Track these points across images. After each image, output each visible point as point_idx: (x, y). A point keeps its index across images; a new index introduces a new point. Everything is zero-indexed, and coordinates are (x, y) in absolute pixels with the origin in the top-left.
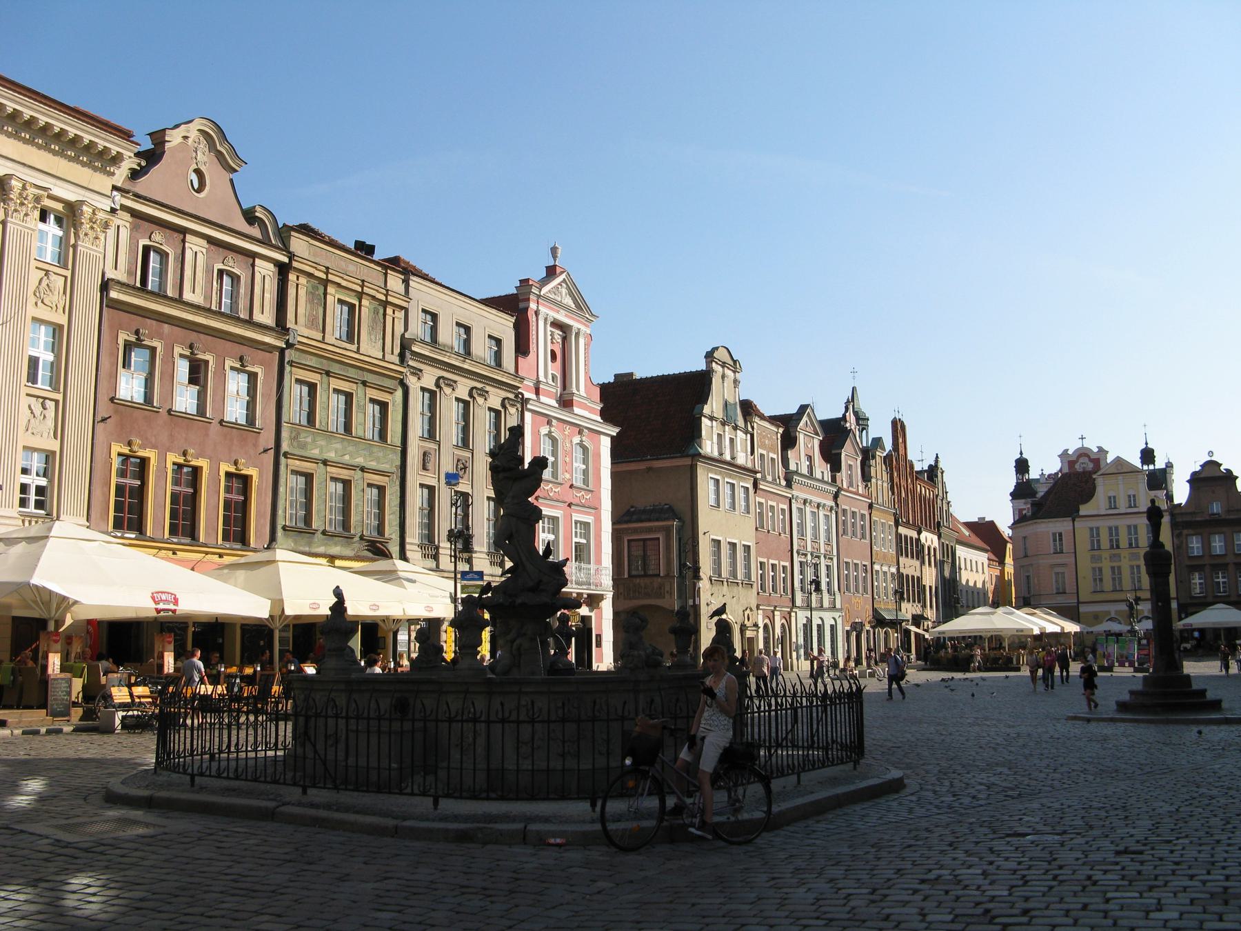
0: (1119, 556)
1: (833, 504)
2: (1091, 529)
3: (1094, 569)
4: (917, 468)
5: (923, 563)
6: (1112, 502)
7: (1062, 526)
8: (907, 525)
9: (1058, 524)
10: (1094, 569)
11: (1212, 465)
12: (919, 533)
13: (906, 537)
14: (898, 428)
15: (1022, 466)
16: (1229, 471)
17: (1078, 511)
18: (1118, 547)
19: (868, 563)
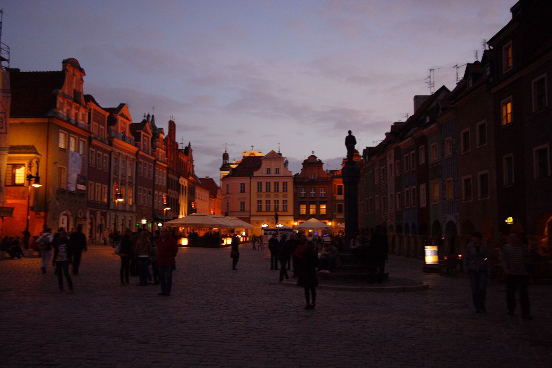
0: (270, 195)
1: (135, 158)
2: (258, 183)
3: (258, 201)
4: (180, 147)
5: (179, 193)
6: (269, 170)
7: (245, 180)
10: (258, 201)
11: (313, 157)
12: (179, 178)
13: (172, 179)
14: (172, 125)
15: (226, 156)
16: (320, 161)
17: (253, 174)
18: (269, 191)
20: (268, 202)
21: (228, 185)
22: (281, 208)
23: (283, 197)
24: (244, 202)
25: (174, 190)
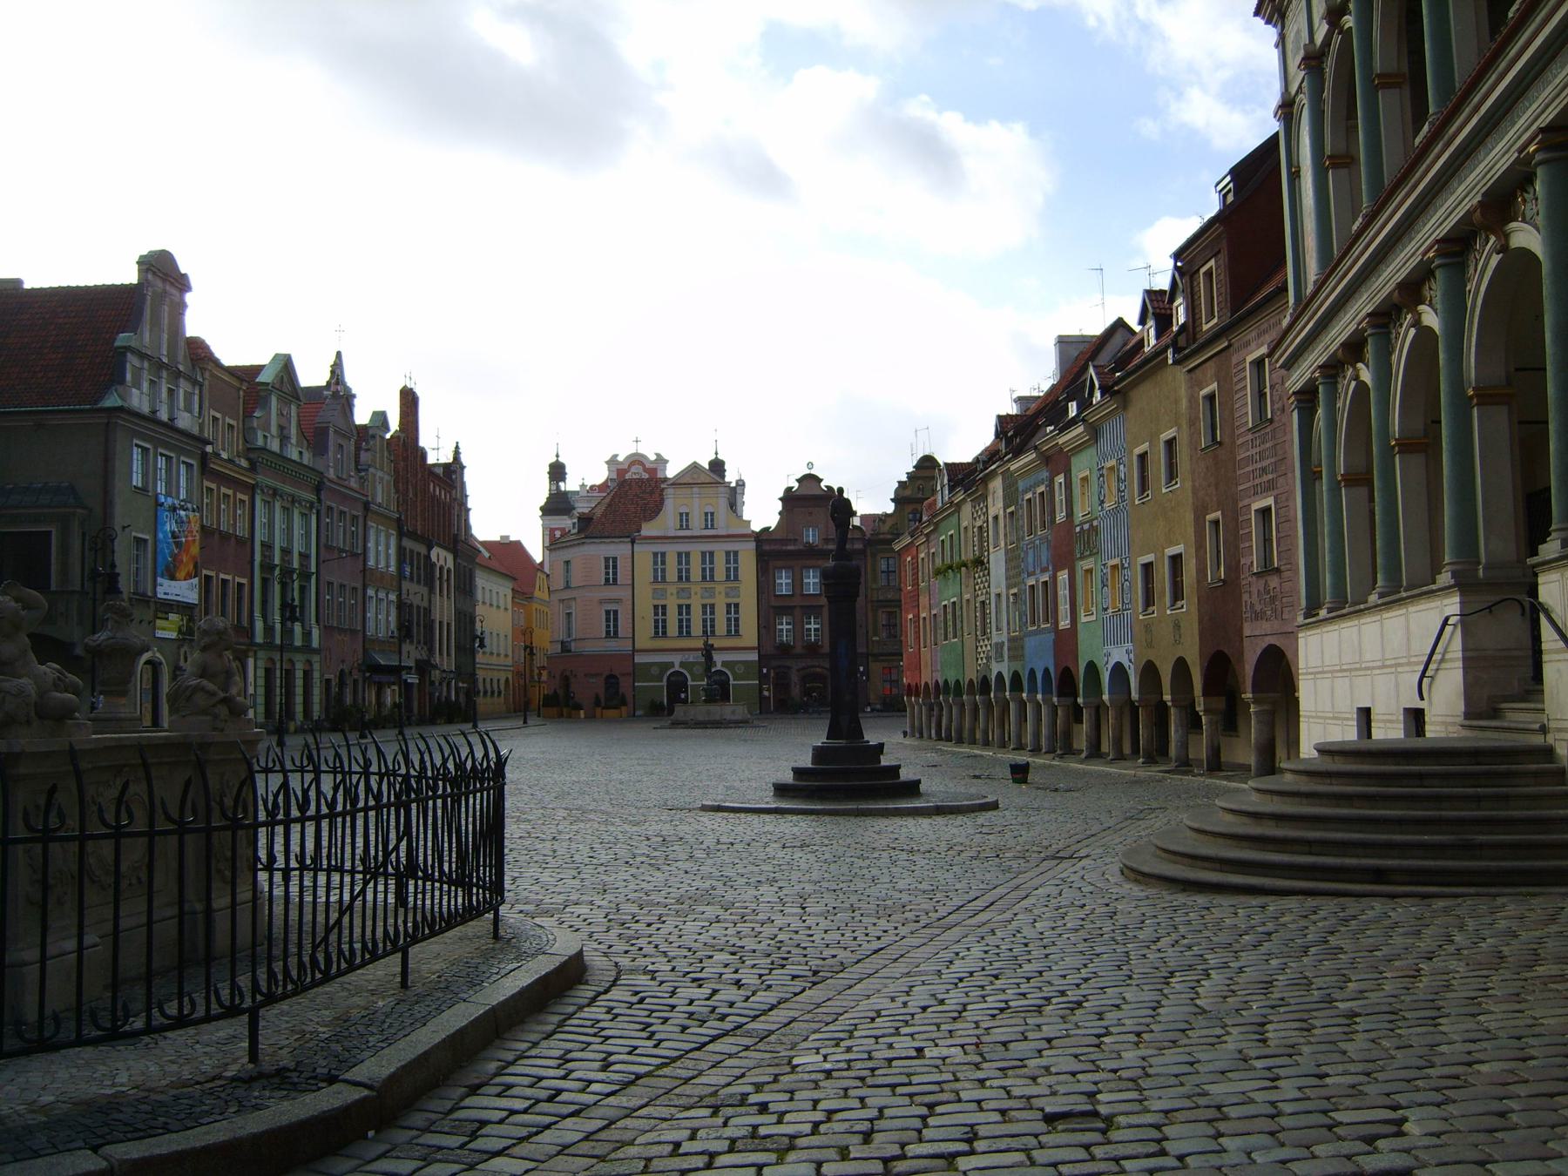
2: (655, 555)
4: (431, 460)
5: (431, 590)
6: (684, 519)
7: (620, 550)
8: (413, 536)
9: (612, 547)
10: (656, 607)
11: (810, 479)
12: (430, 548)
13: (412, 551)
14: (409, 400)
15: (557, 472)
18: (688, 579)
19: (359, 585)
20: (684, 609)
21: (567, 562)
22: (721, 627)
23: (727, 595)
24: (616, 612)
25: (419, 582)
